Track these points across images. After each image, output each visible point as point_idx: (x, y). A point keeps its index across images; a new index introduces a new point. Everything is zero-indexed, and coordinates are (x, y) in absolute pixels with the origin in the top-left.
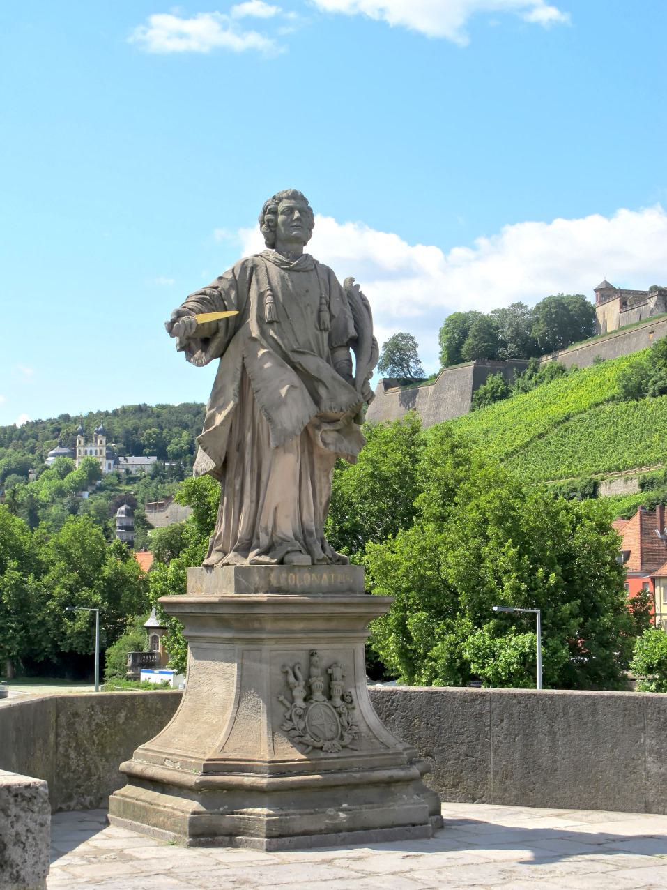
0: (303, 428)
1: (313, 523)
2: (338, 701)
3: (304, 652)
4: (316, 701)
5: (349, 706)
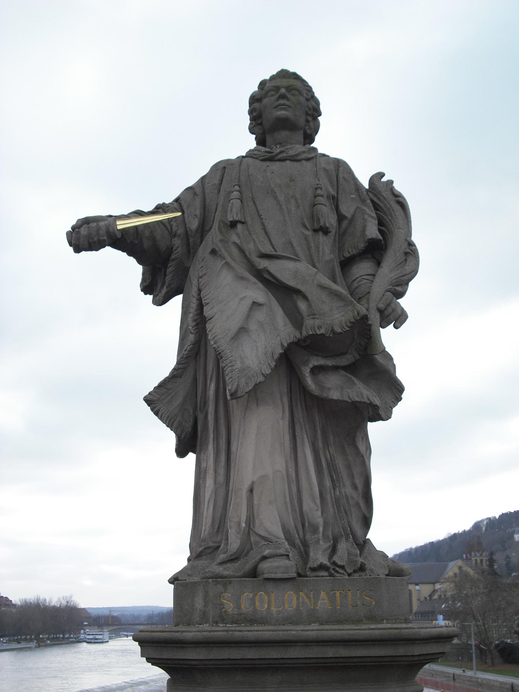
0: (273, 364)
1: (319, 513)
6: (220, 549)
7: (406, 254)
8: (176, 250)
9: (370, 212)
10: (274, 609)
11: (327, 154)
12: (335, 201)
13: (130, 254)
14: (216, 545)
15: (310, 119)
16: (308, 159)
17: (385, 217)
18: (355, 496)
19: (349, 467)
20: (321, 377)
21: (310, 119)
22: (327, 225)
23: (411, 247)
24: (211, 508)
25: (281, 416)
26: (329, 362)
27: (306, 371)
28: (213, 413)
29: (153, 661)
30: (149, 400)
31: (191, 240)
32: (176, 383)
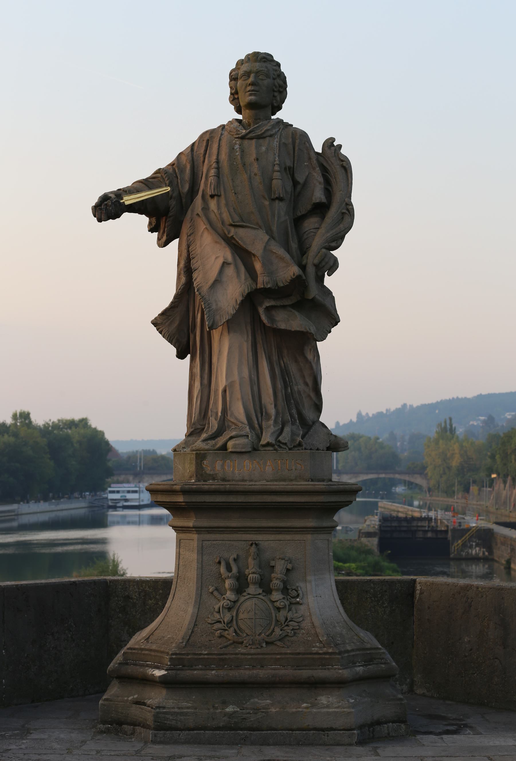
1: (273, 406)
2: (276, 596)
3: (243, 543)
4: (249, 594)
5: (293, 600)
6: (205, 430)
8: (171, 210)
9: (317, 177)
10: (236, 472)
14: (202, 427)
15: (276, 94)
16: (271, 136)
19: (300, 370)
21: (276, 94)
22: (281, 196)
23: (348, 206)
24: (199, 402)
25: (246, 339)
26: (279, 303)
27: (261, 310)
28: (199, 336)
29: (159, 503)
30: (155, 323)
31: (184, 200)
32: (174, 311)
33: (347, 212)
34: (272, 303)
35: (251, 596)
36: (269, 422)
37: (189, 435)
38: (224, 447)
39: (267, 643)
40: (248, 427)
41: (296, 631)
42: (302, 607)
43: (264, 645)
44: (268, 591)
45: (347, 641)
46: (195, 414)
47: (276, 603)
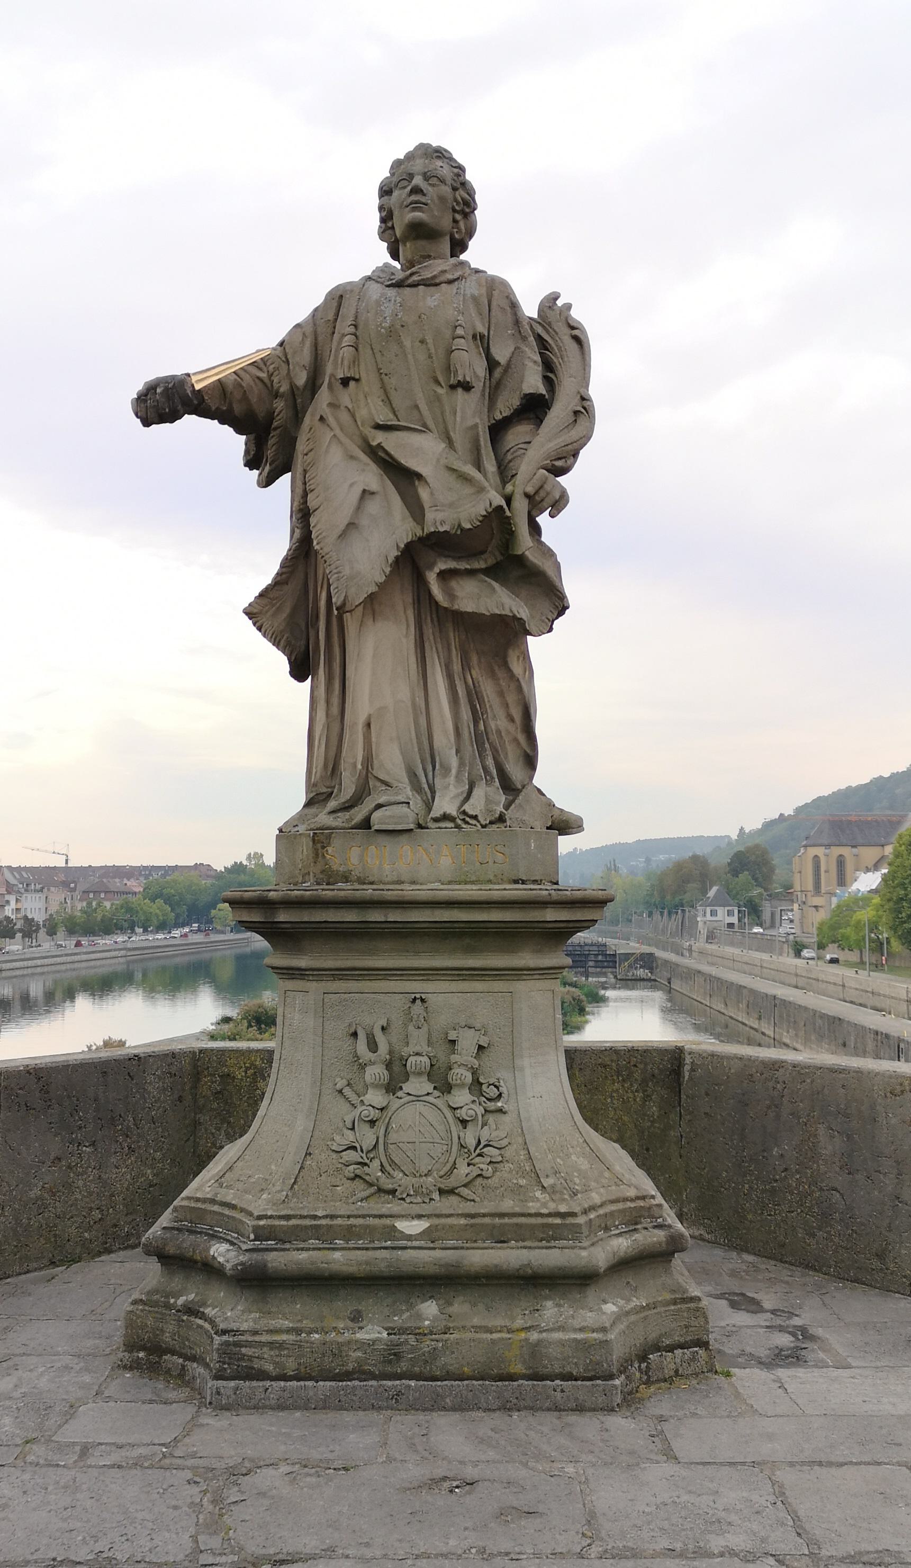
0: (388, 570)
1: (454, 751)
2: (461, 1097)
5: (491, 1106)
7: (576, 413)
8: (278, 415)
9: (532, 354)
10: (386, 867)
11: (481, 268)
12: (483, 341)
13: (222, 422)
14: (329, 790)
15: (458, 217)
16: (450, 282)
17: (555, 360)
18: (511, 728)
19: (501, 694)
20: (453, 583)
21: (458, 217)
22: (468, 379)
24: (323, 746)
25: (405, 633)
26: (463, 565)
27: (431, 577)
28: (324, 630)
29: (247, 925)
30: (250, 613)
31: (299, 401)
33: (583, 410)
34: (452, 564)
35: (411, 1098)
36: (447, 780)
37: (309, 804)
38: (366, 824)
39: (442, 1192)
40: (409, 788)
41: (495, 1165)
42: (506, 1119)
43: (436, 1196)
44: (446, 1088)
45: (593, 1184)
46: (316, 768)
47: (458, 1111)
